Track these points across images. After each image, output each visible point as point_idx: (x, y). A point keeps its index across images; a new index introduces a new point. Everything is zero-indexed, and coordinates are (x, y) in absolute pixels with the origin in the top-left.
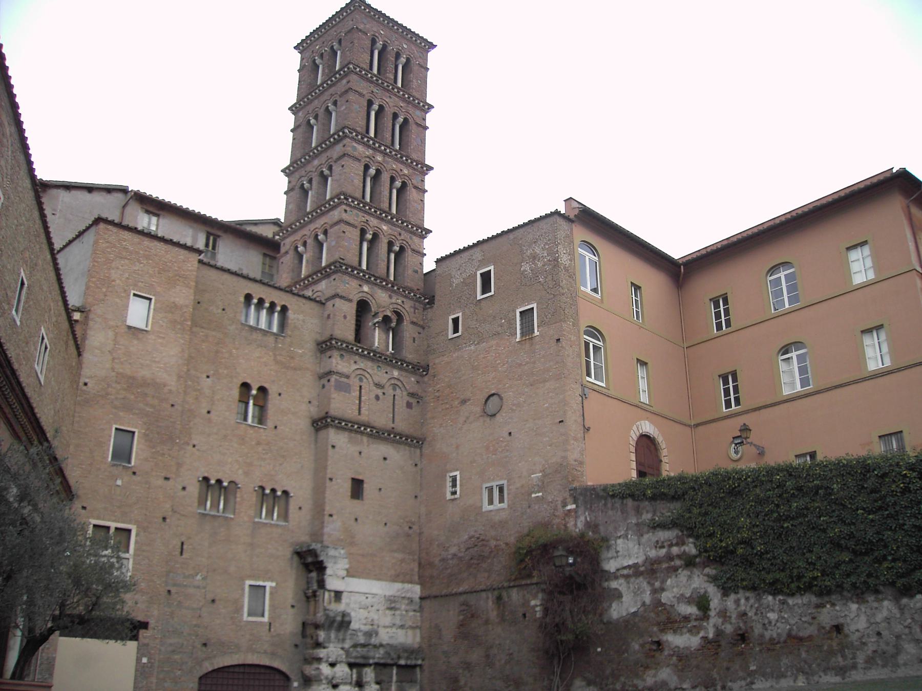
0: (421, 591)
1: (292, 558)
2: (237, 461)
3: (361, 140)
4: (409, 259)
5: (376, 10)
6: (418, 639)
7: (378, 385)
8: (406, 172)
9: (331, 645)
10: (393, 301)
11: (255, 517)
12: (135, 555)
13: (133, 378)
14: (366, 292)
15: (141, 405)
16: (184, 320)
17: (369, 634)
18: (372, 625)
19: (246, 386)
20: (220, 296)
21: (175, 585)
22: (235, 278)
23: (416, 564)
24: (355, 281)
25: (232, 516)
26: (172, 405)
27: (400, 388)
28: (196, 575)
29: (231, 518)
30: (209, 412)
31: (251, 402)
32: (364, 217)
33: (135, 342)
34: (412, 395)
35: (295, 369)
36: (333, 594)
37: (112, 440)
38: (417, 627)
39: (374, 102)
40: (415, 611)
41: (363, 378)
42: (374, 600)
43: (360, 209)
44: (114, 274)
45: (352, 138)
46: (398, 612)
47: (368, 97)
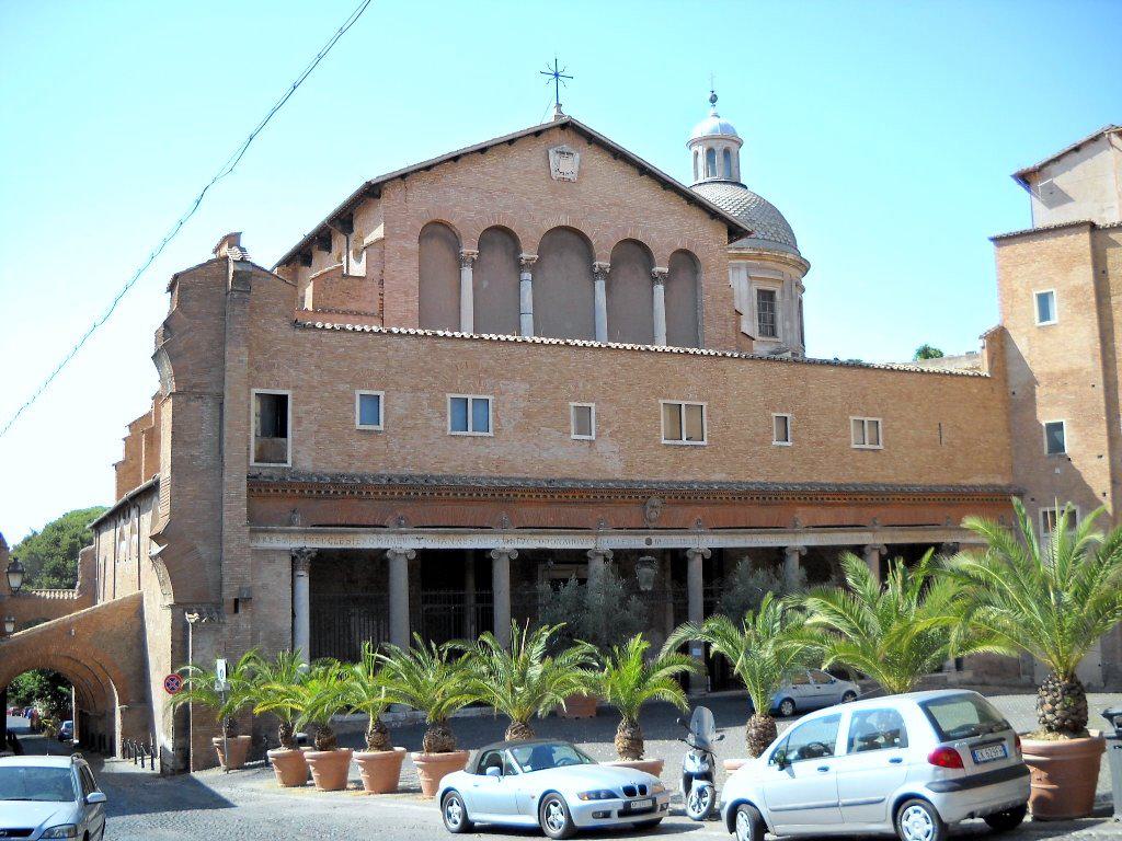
13: (1052, 374)
15: (1063, 395)
33: (1047, 339)
37: (1045, 438)
44: (1016, 284)
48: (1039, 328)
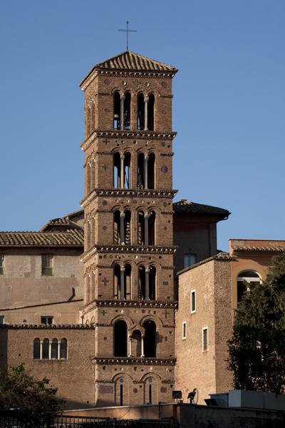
10: (146, 314)
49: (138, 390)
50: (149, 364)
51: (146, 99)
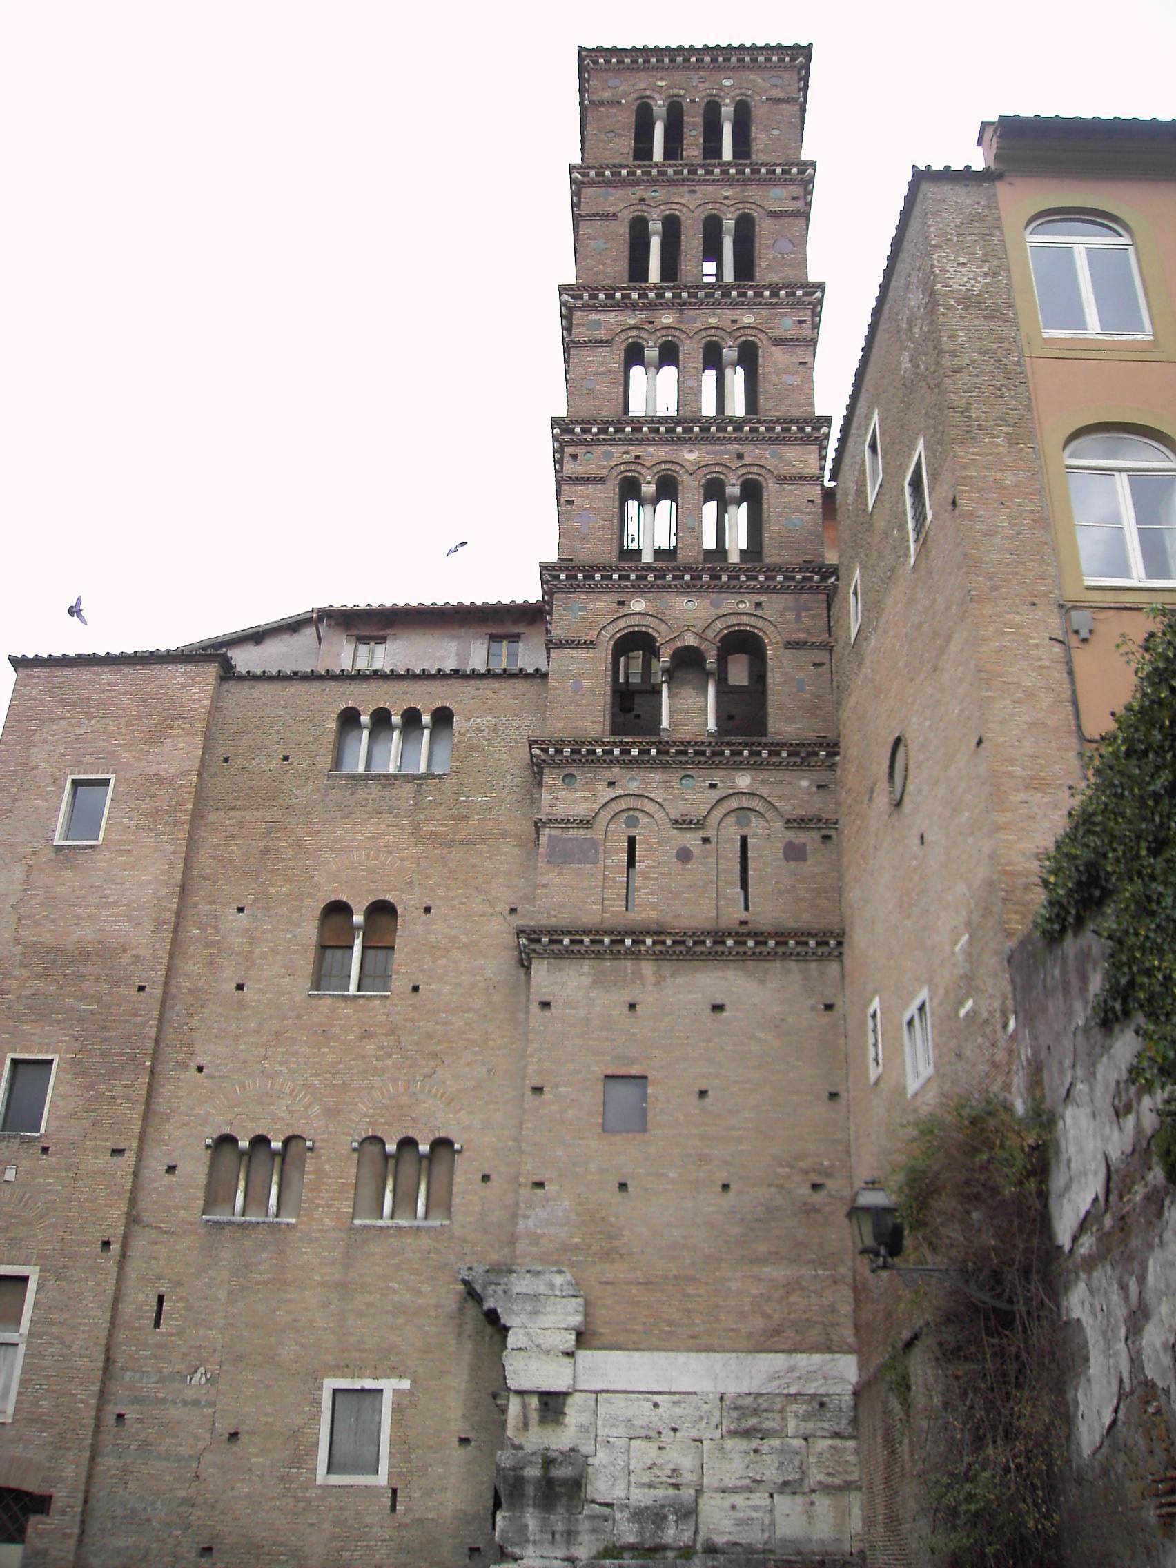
0: (860, 1369)
1: (461, 1310)
2: (308, 1086)
3: (609, 302)
4: (772, 502)
5: (634, 49)
6: (856, 1524)
7: (682, 824)
8: (748, 319)
9: (530, 1550)
10: (725, 610)
11: (353, 1217)
12: (31, 1334)
13: (58, 949)
14: (639, 613)
15: (70, 1001)
16: (178, 804)
17: (652, 1516)
18: (676, 1486)
19: (337, 910)
20: (278, 732)
21: (135, 1400)
22: (315, 687)
23: (847, 1292)
24: (605, 597)
25: (293, 1221)
26: (141, 989)
27: (761, 815)
28: (192, 1375)
29: (288, 1224)
30: (240, 987)
31: (358, 944)
32: (626, 453)
33: (67, 874)
34: (799, 823)
35: (468, 842)
36: (534, 1402)
38: (847, 1487)
39: (649, 217)
40: (836, 1435)
41: (640, 815)
42: (678, 1411)
43: (612, 441)
44: (36, 755)
45: (586, 307)
46: (766, 1446)
47: (627, 215)
48: (59, 849)
49: (696, 851)
50: (736, 765)
51: (727, 110)
